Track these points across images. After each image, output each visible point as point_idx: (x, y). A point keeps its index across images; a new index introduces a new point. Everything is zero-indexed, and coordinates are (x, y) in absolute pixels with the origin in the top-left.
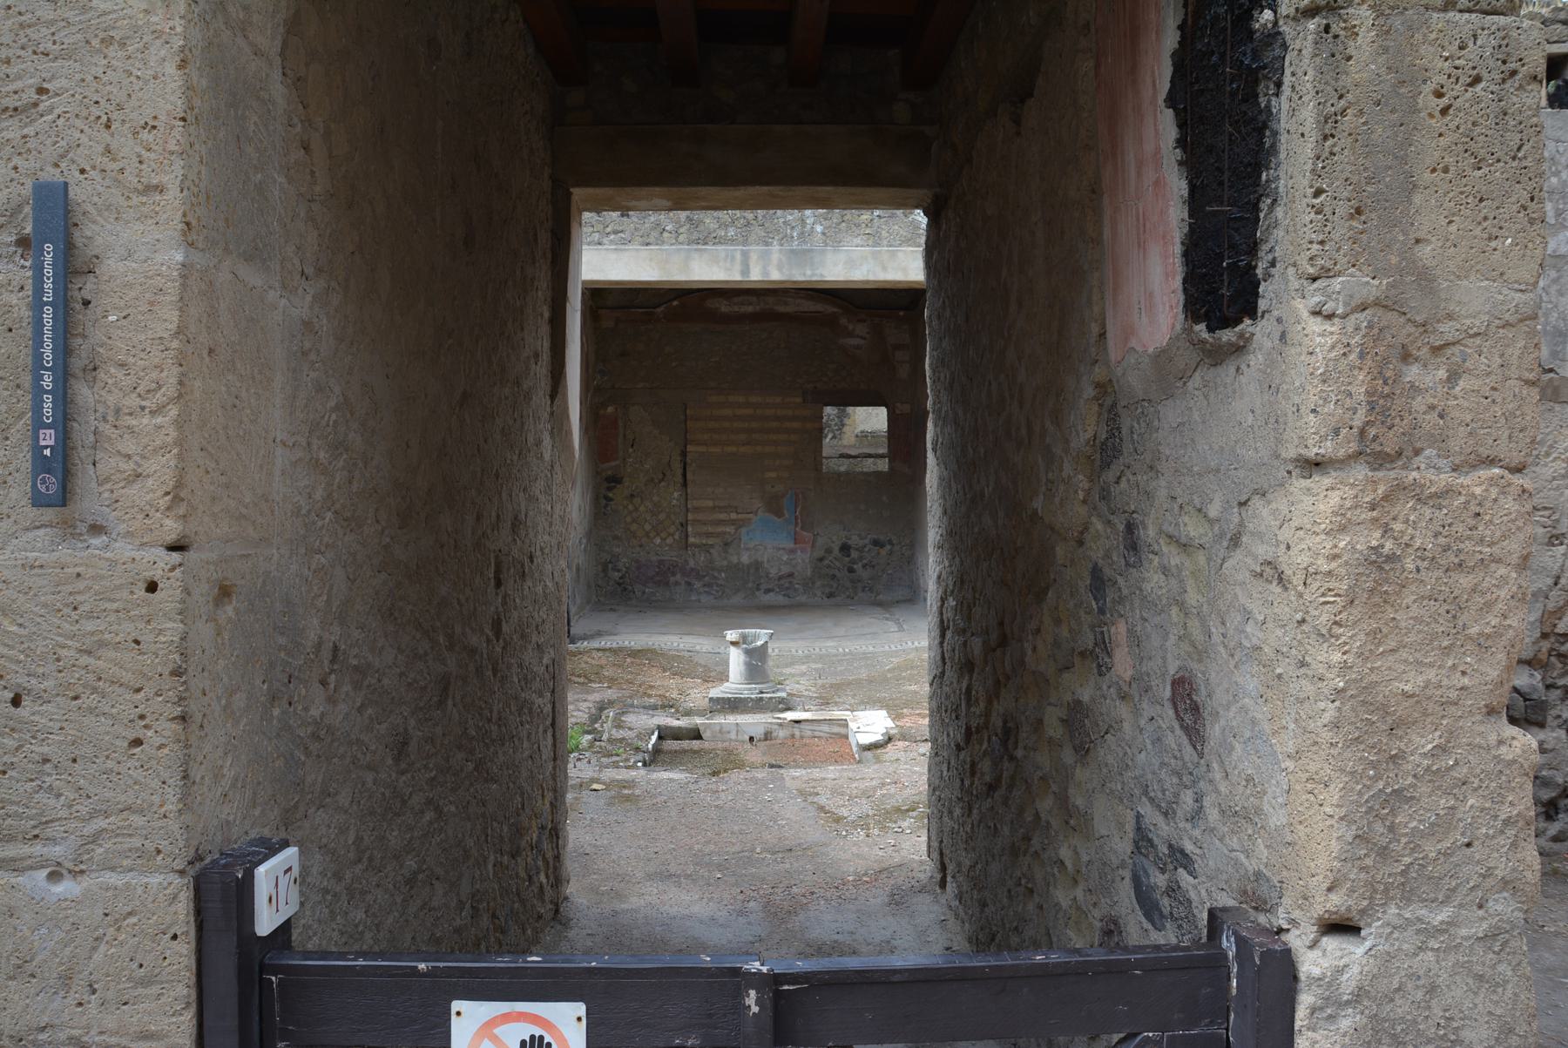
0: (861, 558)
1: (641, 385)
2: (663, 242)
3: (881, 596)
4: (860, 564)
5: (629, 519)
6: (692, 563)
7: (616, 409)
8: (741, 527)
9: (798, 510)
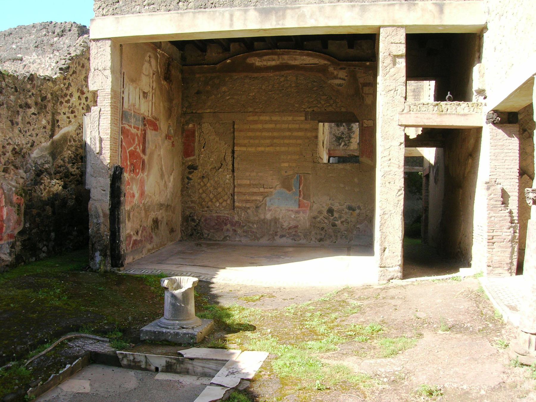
0: (340, 217)
1: (208, 111)
2: (179, 9)
3: (352, 241)
4: (339, 222)
5: (201, 191)
6: (236, 218)
8: (266, 197)
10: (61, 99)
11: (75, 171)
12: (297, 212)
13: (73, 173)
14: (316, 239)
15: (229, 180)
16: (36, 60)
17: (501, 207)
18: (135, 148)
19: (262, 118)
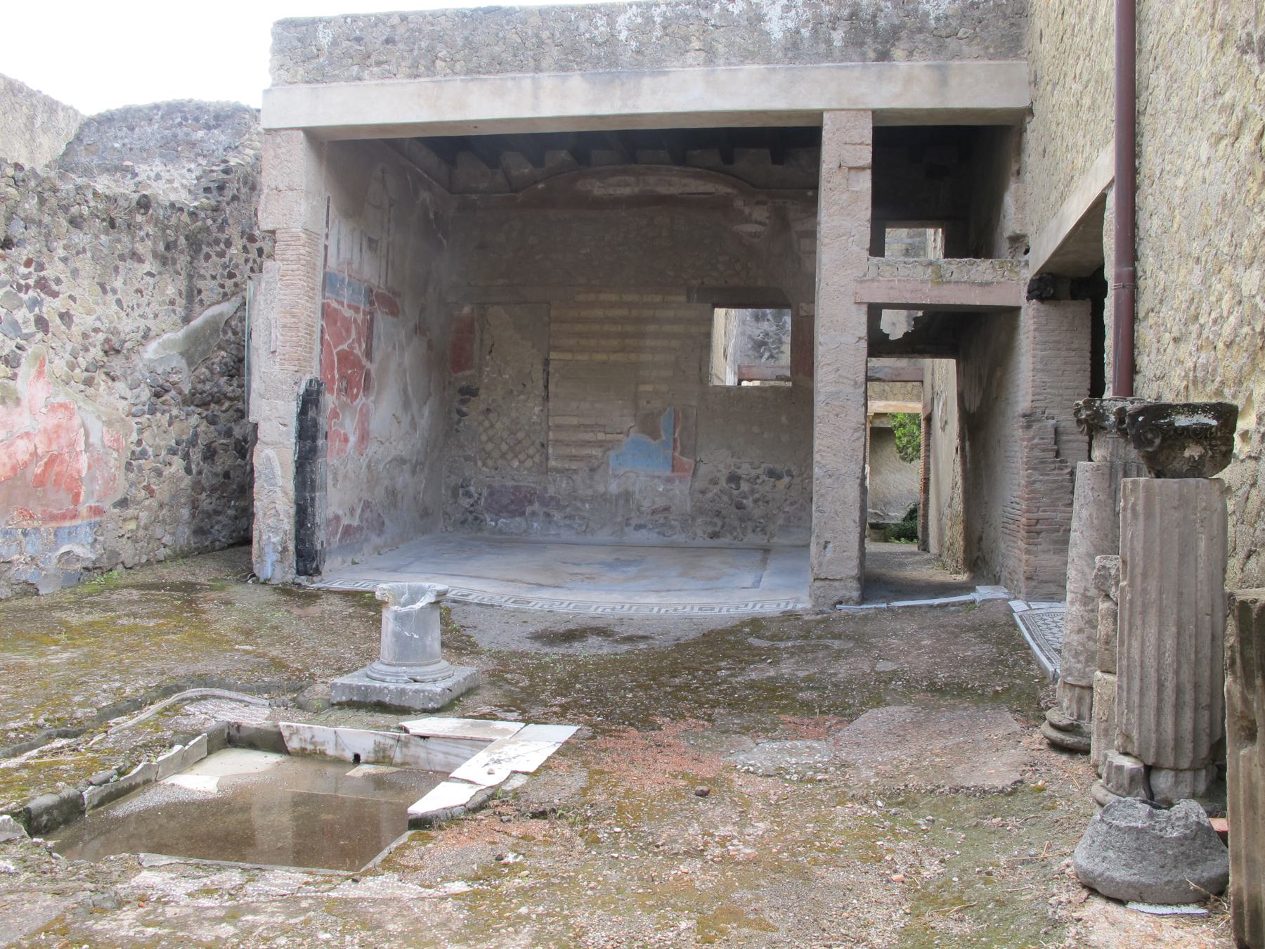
5: (484, 438)
6: (552, 490)
7: (473, 310)
8: (609, 449)
9: (677, 431)
10: (205, 249)
11: (233, 391)
12: (669, 480)
13: (228, 395)
14: (704, 532)
15: (538, 416)
16: (162, 174)
17: (1054, 462)
18: (351, 347)
19: (603, 297)
